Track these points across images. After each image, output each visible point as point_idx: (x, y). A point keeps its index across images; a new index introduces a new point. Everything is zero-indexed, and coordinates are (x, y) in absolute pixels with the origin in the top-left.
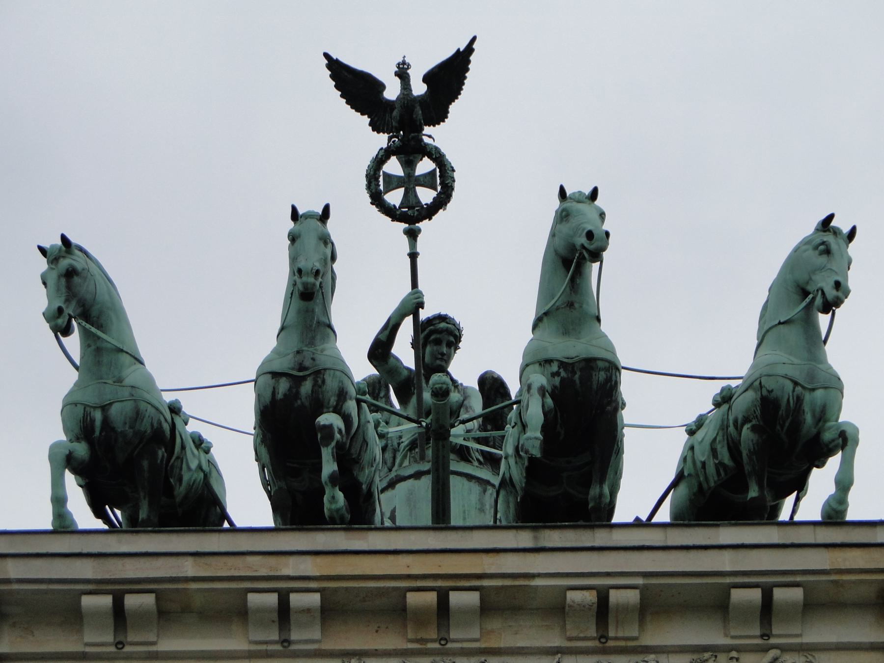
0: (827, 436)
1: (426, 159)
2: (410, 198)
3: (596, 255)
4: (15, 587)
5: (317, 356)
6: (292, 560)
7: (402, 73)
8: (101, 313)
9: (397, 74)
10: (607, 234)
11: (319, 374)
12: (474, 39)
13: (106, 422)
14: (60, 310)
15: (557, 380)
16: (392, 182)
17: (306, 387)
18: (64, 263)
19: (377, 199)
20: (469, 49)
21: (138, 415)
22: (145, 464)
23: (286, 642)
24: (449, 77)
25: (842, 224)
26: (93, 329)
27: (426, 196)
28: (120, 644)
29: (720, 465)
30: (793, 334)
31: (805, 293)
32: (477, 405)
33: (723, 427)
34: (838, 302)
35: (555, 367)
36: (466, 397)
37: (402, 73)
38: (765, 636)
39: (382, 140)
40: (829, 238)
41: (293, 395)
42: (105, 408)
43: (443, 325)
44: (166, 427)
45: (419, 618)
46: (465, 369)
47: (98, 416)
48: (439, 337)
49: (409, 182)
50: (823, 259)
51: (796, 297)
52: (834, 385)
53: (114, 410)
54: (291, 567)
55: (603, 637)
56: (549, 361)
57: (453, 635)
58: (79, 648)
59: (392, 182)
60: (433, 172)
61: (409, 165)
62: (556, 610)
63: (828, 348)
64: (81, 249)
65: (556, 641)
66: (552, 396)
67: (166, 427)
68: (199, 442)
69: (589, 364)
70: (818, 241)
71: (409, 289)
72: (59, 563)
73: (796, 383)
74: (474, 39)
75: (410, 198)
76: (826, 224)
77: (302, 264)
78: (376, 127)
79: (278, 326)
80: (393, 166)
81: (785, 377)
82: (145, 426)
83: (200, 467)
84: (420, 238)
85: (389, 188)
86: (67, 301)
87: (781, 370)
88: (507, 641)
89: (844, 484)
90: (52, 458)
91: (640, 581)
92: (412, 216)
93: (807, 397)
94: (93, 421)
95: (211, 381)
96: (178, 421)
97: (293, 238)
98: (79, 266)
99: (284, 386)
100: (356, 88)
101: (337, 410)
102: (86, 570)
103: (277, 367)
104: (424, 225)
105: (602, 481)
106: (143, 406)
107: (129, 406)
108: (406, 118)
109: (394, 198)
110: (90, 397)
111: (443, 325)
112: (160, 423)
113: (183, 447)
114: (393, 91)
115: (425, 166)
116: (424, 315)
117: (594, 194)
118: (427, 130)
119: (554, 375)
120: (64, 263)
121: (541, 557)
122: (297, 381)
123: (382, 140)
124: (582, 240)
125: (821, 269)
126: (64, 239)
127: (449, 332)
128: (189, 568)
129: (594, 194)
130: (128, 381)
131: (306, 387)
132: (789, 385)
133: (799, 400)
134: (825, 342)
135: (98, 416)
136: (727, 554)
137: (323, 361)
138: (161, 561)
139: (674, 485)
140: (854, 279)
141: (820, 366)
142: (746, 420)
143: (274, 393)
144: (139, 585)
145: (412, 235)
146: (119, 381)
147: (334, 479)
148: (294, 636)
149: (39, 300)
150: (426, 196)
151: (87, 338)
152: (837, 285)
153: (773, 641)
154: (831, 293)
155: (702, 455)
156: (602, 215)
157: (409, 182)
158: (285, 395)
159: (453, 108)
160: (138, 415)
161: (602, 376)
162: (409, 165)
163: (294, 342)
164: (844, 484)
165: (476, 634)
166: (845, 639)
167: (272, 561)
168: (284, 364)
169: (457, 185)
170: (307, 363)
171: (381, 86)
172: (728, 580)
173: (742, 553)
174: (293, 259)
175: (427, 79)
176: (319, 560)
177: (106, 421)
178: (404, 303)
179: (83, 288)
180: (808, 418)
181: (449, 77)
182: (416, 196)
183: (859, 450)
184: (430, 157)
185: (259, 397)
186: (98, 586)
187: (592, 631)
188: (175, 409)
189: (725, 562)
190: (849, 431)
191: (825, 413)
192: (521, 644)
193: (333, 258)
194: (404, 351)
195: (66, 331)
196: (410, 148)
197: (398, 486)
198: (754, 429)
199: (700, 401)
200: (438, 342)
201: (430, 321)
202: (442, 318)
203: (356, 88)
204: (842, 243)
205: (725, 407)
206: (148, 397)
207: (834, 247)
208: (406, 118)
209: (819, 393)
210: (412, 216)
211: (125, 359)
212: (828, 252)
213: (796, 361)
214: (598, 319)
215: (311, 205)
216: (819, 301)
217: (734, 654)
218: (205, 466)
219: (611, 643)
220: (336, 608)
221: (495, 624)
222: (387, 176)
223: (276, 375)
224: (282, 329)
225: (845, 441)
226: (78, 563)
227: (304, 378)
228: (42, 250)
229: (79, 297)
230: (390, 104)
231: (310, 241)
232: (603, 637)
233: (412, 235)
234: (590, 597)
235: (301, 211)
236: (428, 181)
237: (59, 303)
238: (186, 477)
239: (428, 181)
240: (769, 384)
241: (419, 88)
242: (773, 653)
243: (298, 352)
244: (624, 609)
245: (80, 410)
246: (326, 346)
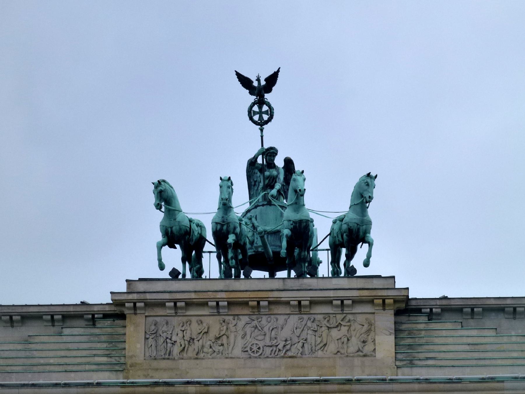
0: (366, 239)
1: (265, 105)
2: (261, 118)
3: (302, 195)
4: (149, 301)
5: (228, 219)
6: (219, 293)
7: (258, 80)
8: (170, 199)
9: (256, 80)
10: (305, 190)
11: (228, 224)
12: (280, 68)
13: (172, 231)
14: (158, 204)
15: (292, 226)
16: (255, 113)
17: (225, 227)
18: (160, 188)
19: (251, 119)
20: (278, 71)
21: (180, 229)
22: (183, 242)
23: (218, 312)
24: (272, 80)
25: (373, 174)
26: (168, 207)
27: (266, 117)
28: (176, 313)
29: (339, 240)
30: (358, 208)
31: (362, 196)
32: (282, 177)
33: (340, 229)
34: (370, 202)
35: (291, 222)
36: (279, 173)
37: (258, 80)
38: (342, 310)
39: (253, 98)
40: (369, 180)
41: (221, 229)
42: (171, 228)
43: (272, 151)
44: (188, 229)
45: (253, 307)
46: (279, 162)
47: (170, 230)
48: (270, 153)
49: (261, 113)
50: (366, 187)
51: (359, 196)
52: (369, 223)
53: (174, 228)
54: (220, 295)
55: (300, 311)
56: (290, 221)
57: (262, 310)
58: (166, 314)
59: (255, 113)
60: (267, 111)
61: (260, 108)
62: (287, 303)
63: (369, 210)
64: (164, 181)
65: (288, 312)
66: (291, 230)
67: (188, 229)
68: (198, 225)
69: (301, 221)
70: (365, 181)
71: (260, 147)
72: (160, 294)
73: (358, 225)
74: (280, 68)
75: (261, 118)
76: (369, 175)
77: (223, 197)
78: (251, 93)
79: (217, 207)
80: (256, 108)
81: (355, 223)
82: (183, 232)
83: (198, 233)
84: (264, 130)
85: (254, 115)
86: (160, 200)
87: (354, 221)
88: (276, 312)
89: (369, 256)
90: (157, 247)
91: (309, 299)
92: (261, 124)
93: (361, 228)
94: (168, 231)
95: (200, 209)
96: (192, 224)
97: (221, 187)
98: (163, 189)
99: (219, 227)
100: (245, 82)
101: (233, 233)
102: (167, 296)
103: (217, 221)
104: (265, 126)
105: (305, 251)
106: (181, 227)
107: (178, 228)
108: (260, 90)
109: (256, 118)
110: (168, 225)
111: (272, 151)
112: (186, 230)
113: (193, 232)
114: (255, 84)
115: (265, 108)
116: (266, 146)
117: (303, 172)
118: (266, 96)
119: (291, 224)
120: (160, 188)
121: (284, 292)
122: (222, 225)
123: (253, 98)
124: (298, 191)
125: (366, 190)
126: (158, 181)
127: (274, 153)
128: (193, 296)
129: (303, 172)
130: (178, 220)
131: (225, 227)
132: (356, 225)
133: (359, 229)
134: (368, 208)
135: (170, 230)
136: (332, 292)
137: (230, 220)
138: (186, 294)
139: (330, 234)
140: (374, 195)
141: (365, 218)
142: (345, 232)
143: (216, 228)
144: (180, 300)
145: (262, 130)
146: (175, 219)
147: (232, 258)
148: (221, 311)
149: (152, 199)
150: (266, 117)
151: (166, 208)
152: (370, 197)
153: (344, 312)
154: (368, 199)
155: (335, 235)
156: (304, 180)
157: (261, 113)
158: (219, 229)
159: (274, 88)
160: (180, 229)
161: (305, 224)
162: (260, 108)
163: (221, 214)
164: (369, 256)
165: (267, 310)
166: (363, 312)
167: (214, 293)
168: (219, 220)
169: (275, 114)
170: (225, 220)
171: (253, 82)
172: (332, 299)
173: (335, 291)
174: (221, 193)
175: (265, 80)
176: (226, 293)
177: (172, 231)
178: (259, 151)
179: (164, 195)
180: (361, 234)
181: (272, 80)
182: (263, 118)
183: (373, 247)
184: (266, 105)
185: (212, 228)
186: (170, 300)
187: (297, 310)
188: (191, 221)
189: (331, 294)
190: (371, 241)
191: (367, 232)
192: (279, 313)
193: (232, 184)
194: (260, 160)
195: (161, 208)
196: (261, 102)
197: (258, 208)
198: (346, 235)
199: (335, 216)
200: (270, 156)
201: (268, 150)
202: (271, 148)
203: (245, 82)
204: (373, 180)
205: (341, 223)
206: (183, 224)
207: (370, 183)
208: (260, 90)
209: (364, 227)
210: (261, 124)
211: (177, 212)
212: (368, 185)
213: (359, 218)
214: (304, 205)
215: (225, 176)
216: (365, 201)
217: (334, 315)
218: (200, 232)
219: (302, 312)
220: (231, 304)
221: (272, 307)
222: (254, 111)
223: (217, 223)
224: (219, 209)
225: (370, 245)
226: (165, 294)
227: (224, 225)
228: (153, 184)
229: (164, 197)
230: (255, 87)
231: (225, 188)
232: (300, 311)
233: (262, 130)
234: (296, 303)
235: (223, 178)
236: (266, 112)
237: (158, 202)
238: (194, 239)
239: (266, 112)
240: (351, 225)
241: (263, 83)
242: (344, 315)
243: (223, 217)
244: (305, 306)
245: (165, 227)
246: (231, 214)
